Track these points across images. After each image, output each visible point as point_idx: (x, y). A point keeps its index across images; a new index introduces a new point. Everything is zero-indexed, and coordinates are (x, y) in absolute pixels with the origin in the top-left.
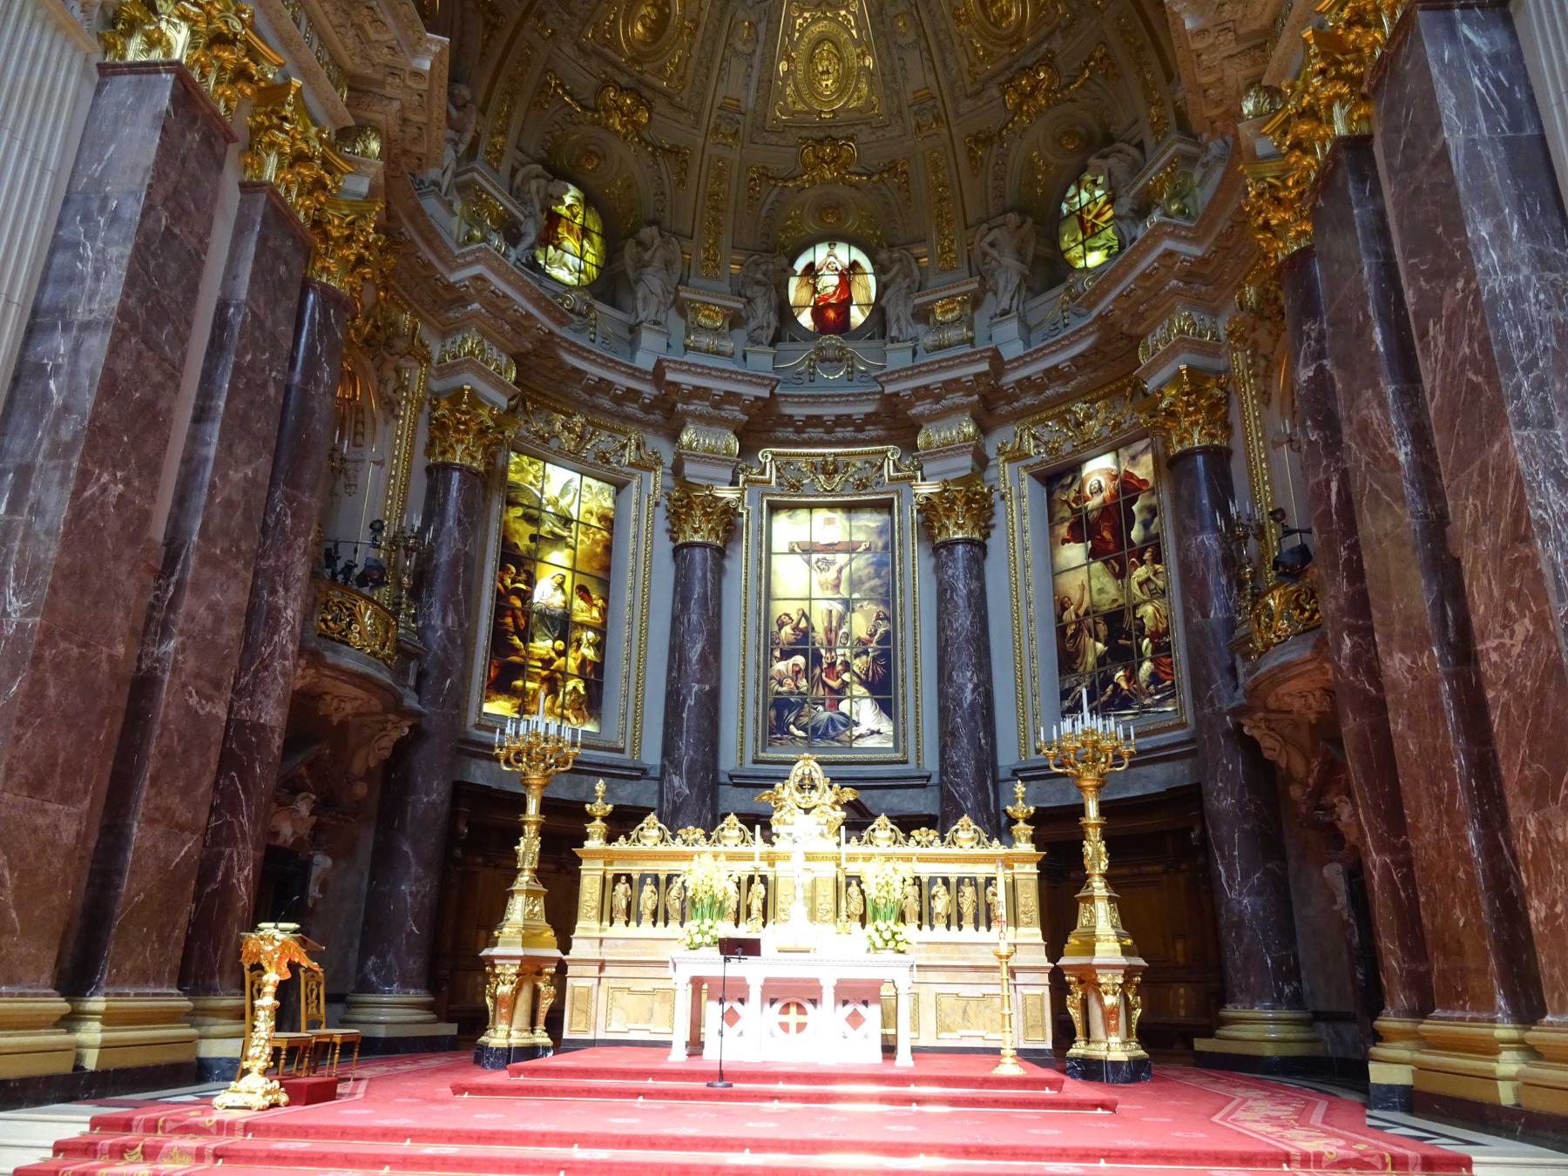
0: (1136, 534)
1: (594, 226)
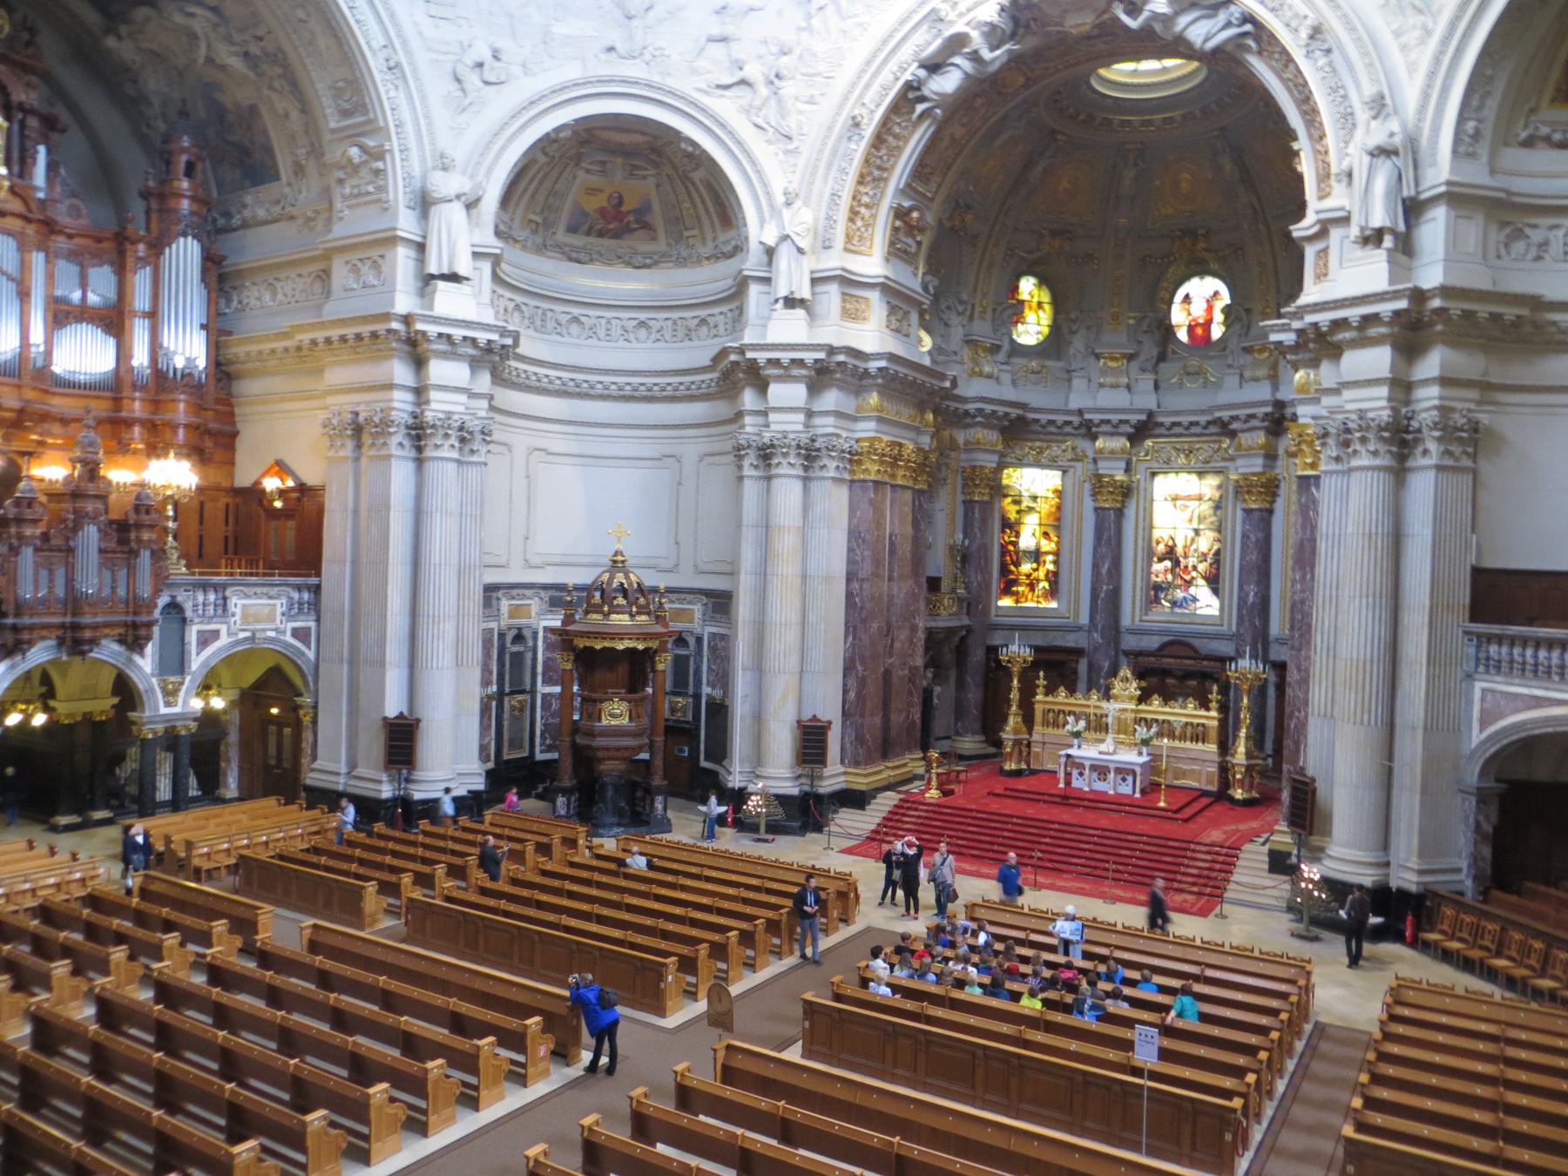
1: (1045, 297)
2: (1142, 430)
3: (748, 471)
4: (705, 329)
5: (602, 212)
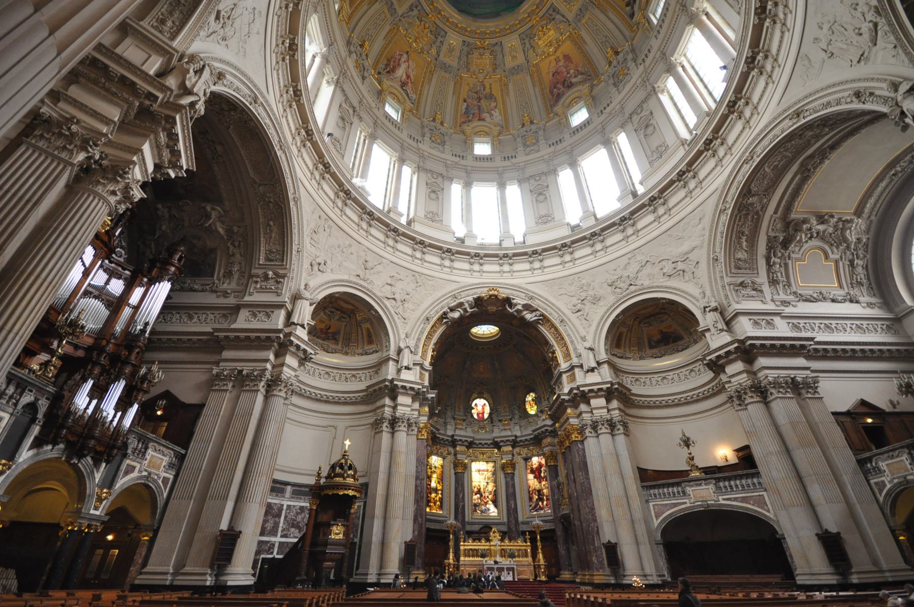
0: (542, 475)
2: (470, 445)
3: (384, 428)
4: (354, 378)
5: (321, 330)
